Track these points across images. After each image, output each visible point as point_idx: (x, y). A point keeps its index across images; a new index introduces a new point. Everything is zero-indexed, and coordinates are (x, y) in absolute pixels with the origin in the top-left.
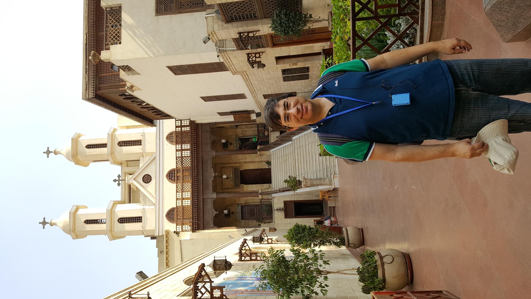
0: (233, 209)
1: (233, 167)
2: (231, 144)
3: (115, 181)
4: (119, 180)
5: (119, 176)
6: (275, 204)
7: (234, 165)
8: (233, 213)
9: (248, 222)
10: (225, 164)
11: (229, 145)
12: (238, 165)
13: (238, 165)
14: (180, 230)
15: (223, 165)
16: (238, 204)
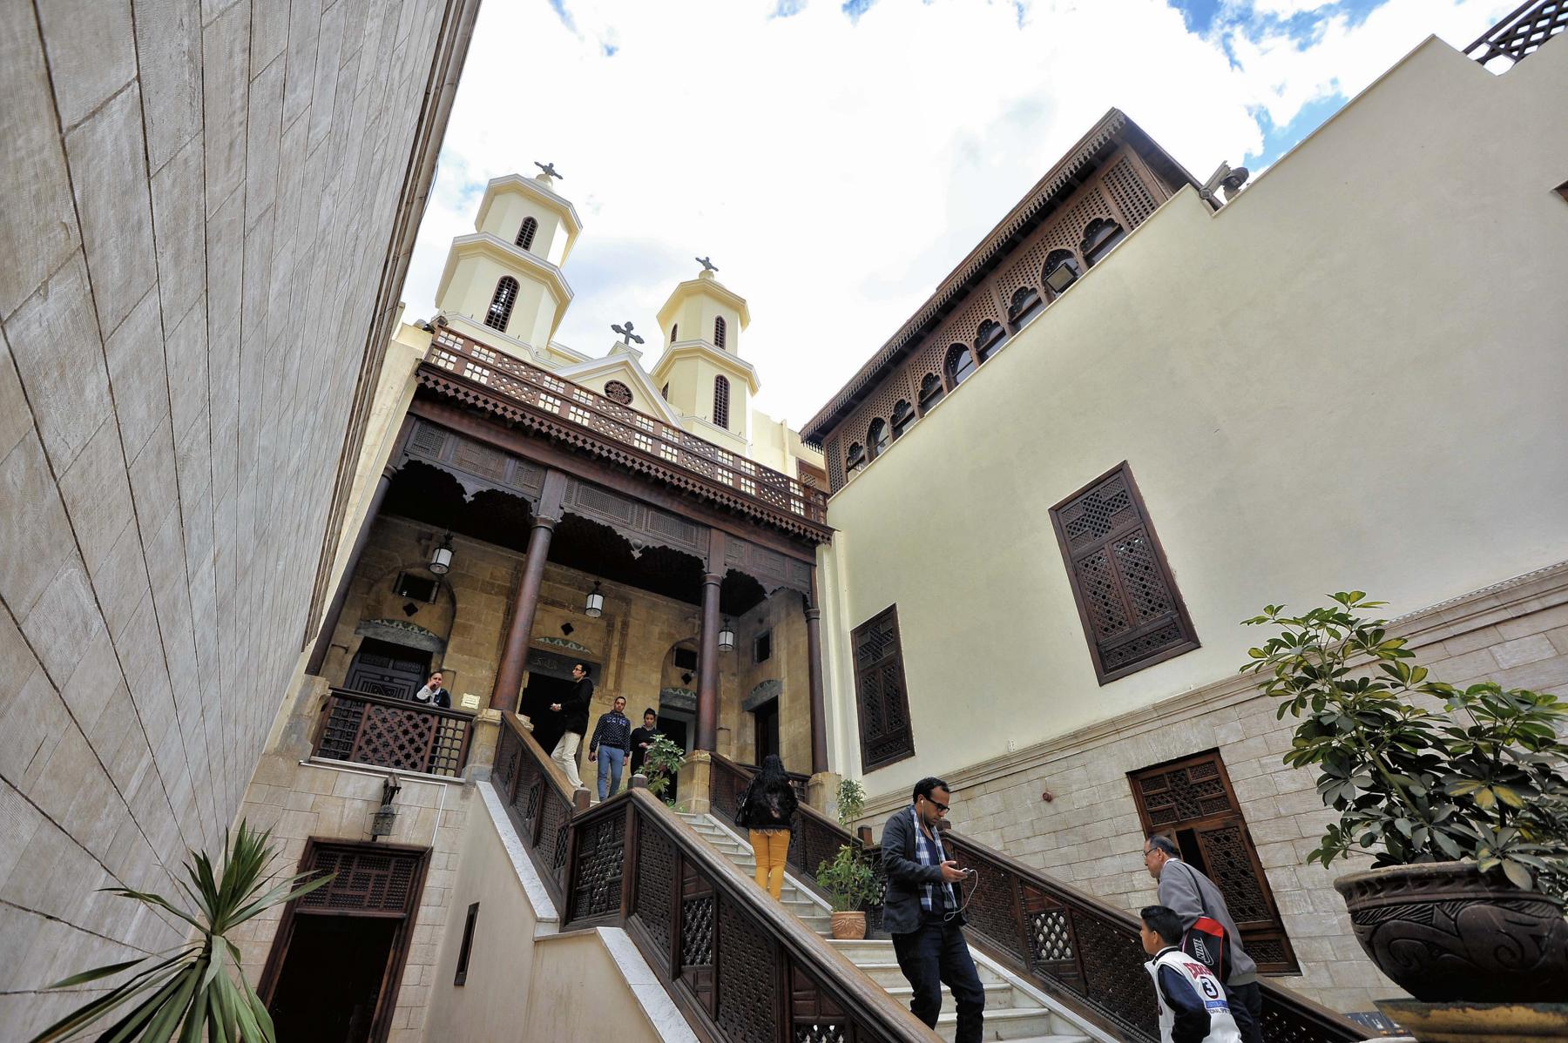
0: (429, 616)
1: (607, 658)
2: (687, 679)
3: (629, 326)
4: (628, 335)
5: (639, 340)
6: (431, 788)
7: (613, 667)
8: (410, 610)
9: (341, 664)
10: (624, 635)
11: (684, 671)
12: (611, 684)
13: (611, 684)
14: (441, 340)
15: (618, 625)
16: (443, 644)
